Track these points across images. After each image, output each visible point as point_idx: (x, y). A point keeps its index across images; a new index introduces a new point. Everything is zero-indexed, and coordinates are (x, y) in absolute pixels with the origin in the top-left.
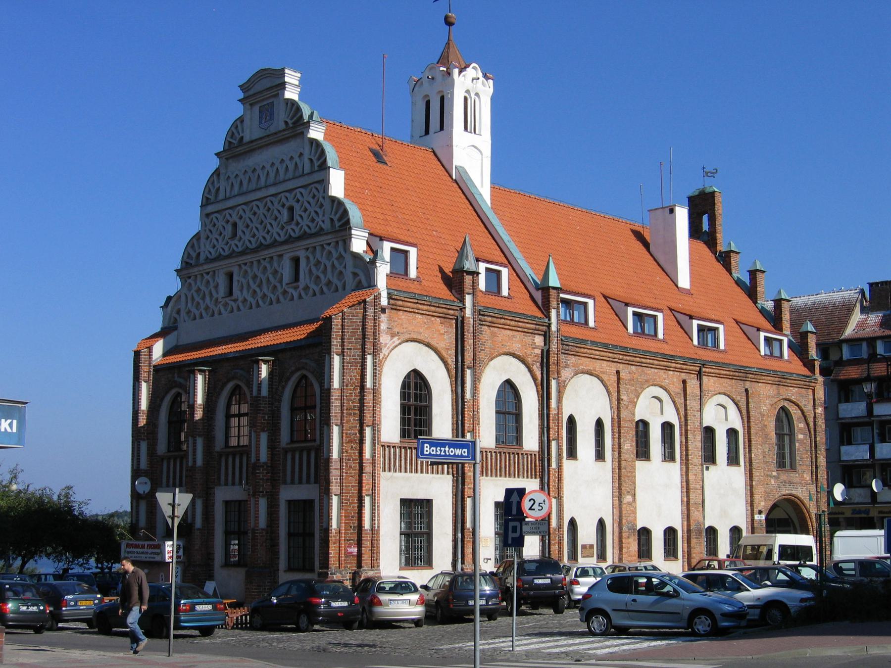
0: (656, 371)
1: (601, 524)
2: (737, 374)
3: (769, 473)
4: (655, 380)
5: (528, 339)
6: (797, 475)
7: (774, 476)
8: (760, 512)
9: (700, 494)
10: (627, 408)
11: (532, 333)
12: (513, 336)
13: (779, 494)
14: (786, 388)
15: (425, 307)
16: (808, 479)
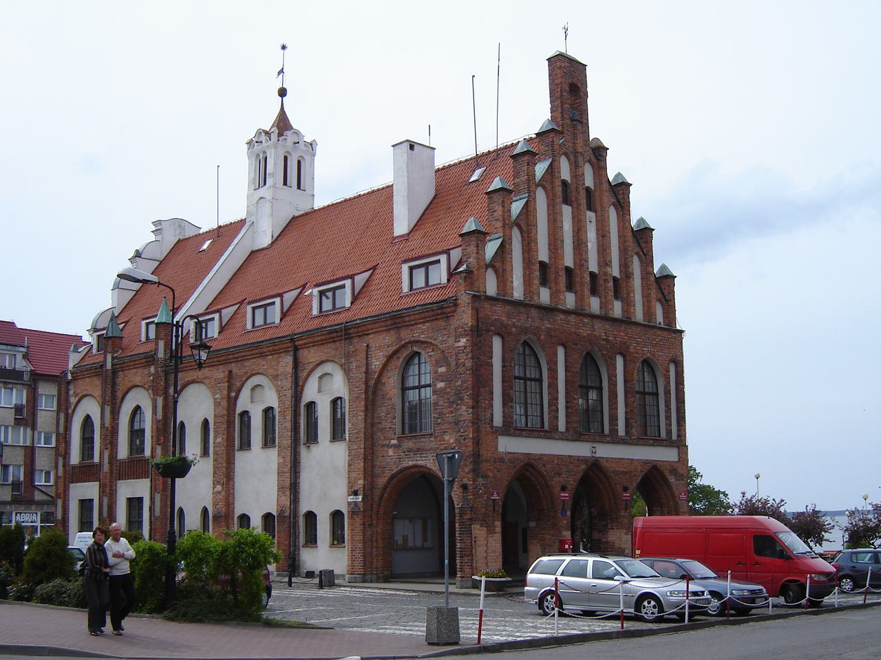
0: (255, 360)
1: (205, 511)
2: (334, 335)
3: (387, 442)
4: (253, 370)
5: (146, 371)
6: (432, 439)
7: (394, 446)
8: (355, 493)
9: (287, 478)
10: (220, 405)
11: (148, 365)
12: (136, 373)
13: (399, 468)
14: (412, 328)
15: (86, 373)
16: (452, 441)
